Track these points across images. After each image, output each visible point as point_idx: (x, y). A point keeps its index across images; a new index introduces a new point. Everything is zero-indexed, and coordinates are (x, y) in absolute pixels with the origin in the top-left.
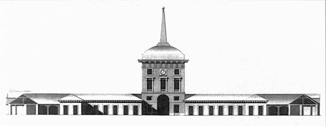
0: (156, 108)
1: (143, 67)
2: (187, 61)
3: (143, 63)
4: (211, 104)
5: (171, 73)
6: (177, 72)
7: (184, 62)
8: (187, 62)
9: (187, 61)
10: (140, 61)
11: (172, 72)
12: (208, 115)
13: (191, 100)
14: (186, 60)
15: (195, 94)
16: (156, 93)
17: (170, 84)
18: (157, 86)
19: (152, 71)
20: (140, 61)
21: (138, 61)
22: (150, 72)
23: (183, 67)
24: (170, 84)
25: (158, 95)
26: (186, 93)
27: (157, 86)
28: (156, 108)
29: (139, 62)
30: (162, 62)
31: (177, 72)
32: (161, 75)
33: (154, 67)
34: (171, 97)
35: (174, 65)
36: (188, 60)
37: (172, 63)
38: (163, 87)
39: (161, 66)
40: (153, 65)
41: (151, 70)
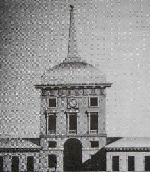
0: (84, 161)
1: (43, 96)
2: (109, 85)
3: (42, 89)
4: (131, 154)
5: (83, 103)
6: (94, 102)
7: (105, 88)
8: (110, 86)
9: (109, 85)
10: (37, 87)
11: (45, 102)
12: (10, 171)
13: (116, 147)
14: (107, 84)
15: (121, 137)
16: (62, 136)
17: (83, 123)
18: (62, 123)
19: (57, 102)
20: (37, 87)
21: (34, 86)
22: (52, 103)
23: (103, 95)
24: (83, 123)
25: (65, 139)
26: (108, 136)
27: (62, 123)
28: (84, 161)
29: (37, 88)
30: (79, 87)
31: (94, 102)
32: (70, 107)
33: (84, 95)
34: (86, 143)
35: (89, 92)
36: (111, 84)
37: (69, 89)
38: (73, 125)
39: (69, 92)
40: (56, 92)
41: (96, 99)
